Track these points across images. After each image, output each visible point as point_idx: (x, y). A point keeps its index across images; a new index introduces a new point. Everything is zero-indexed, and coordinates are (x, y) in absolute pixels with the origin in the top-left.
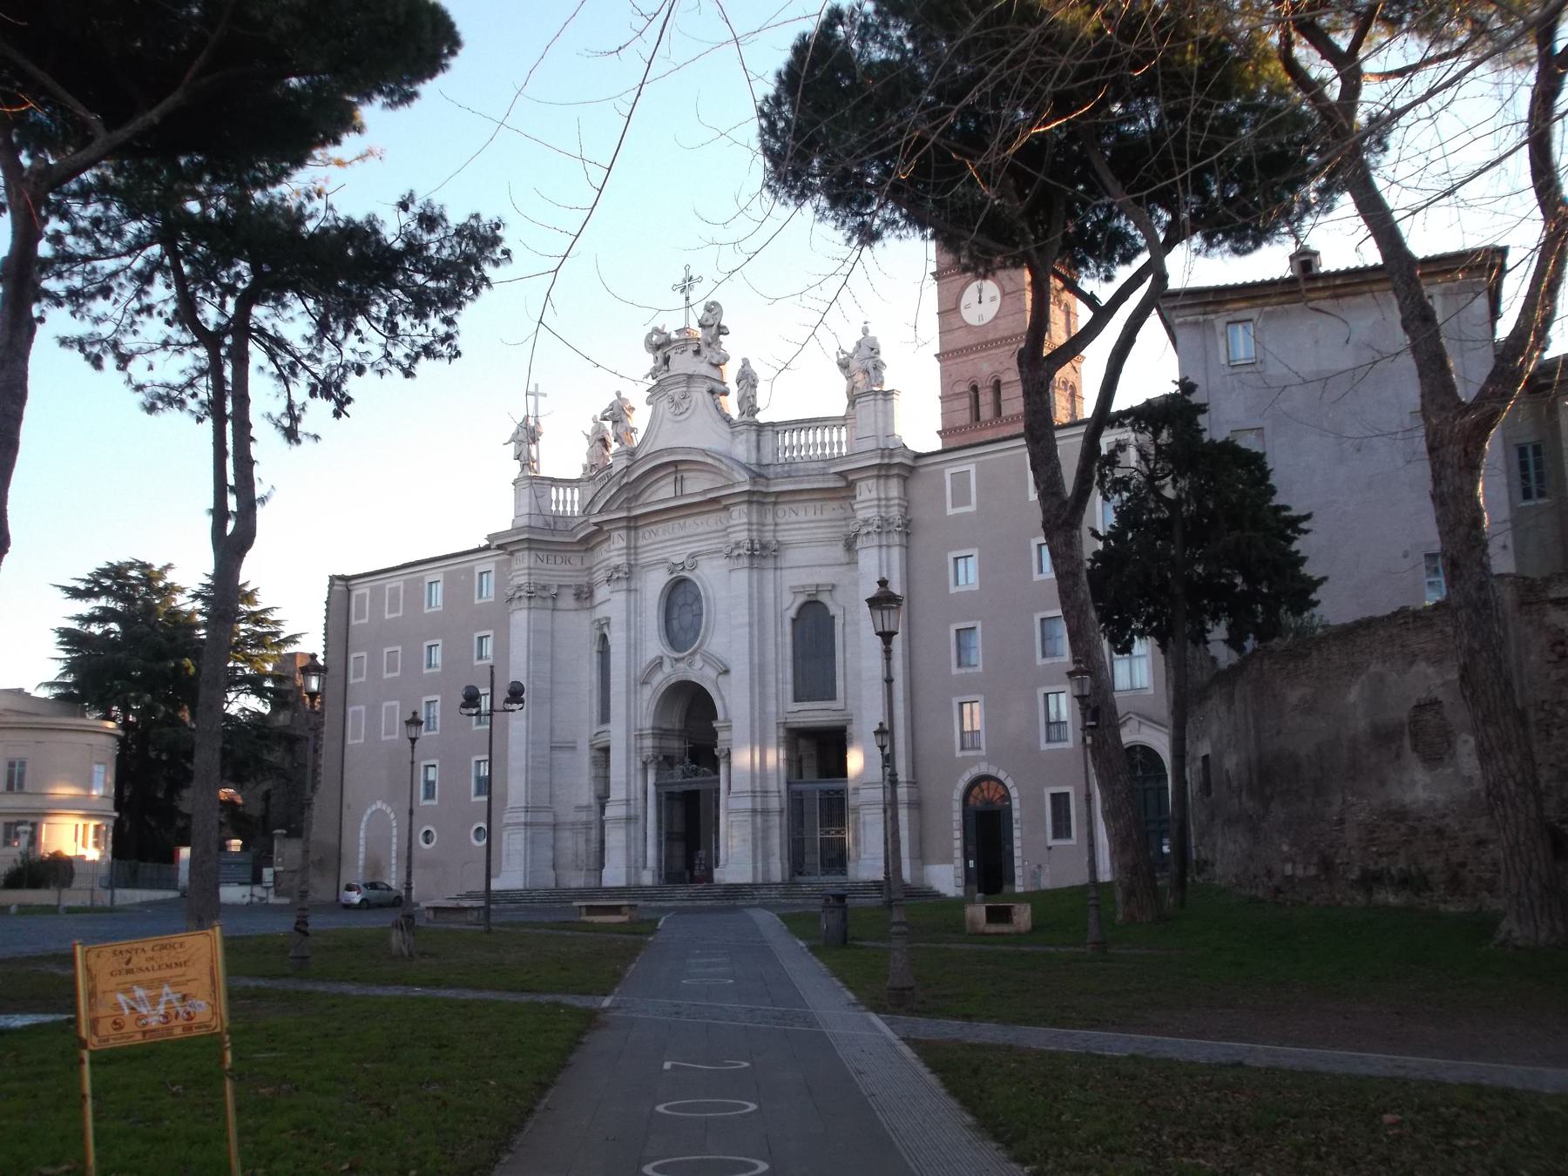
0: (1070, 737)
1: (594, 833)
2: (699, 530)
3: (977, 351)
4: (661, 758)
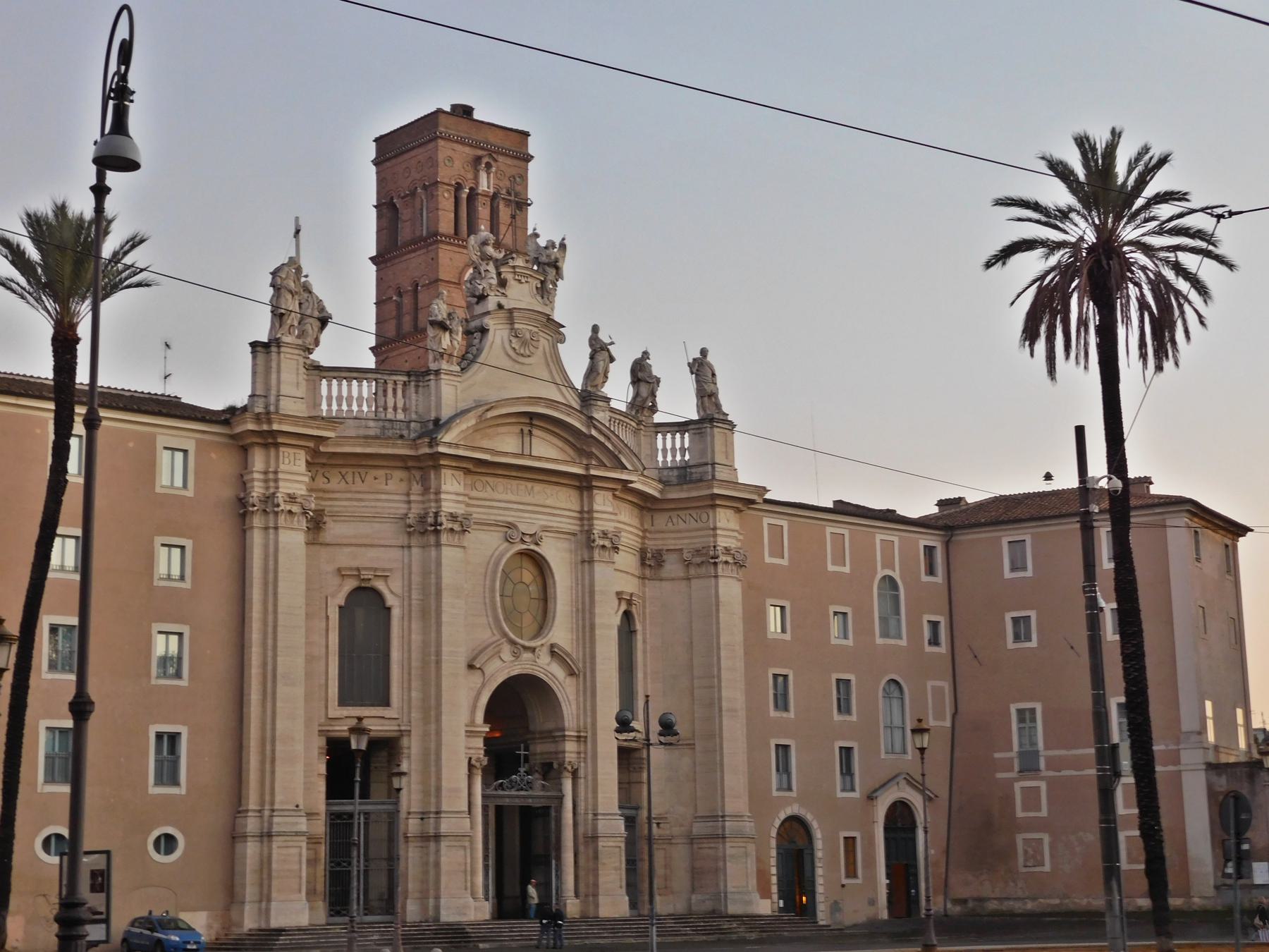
0: (857, 787)
2: (548, 502)
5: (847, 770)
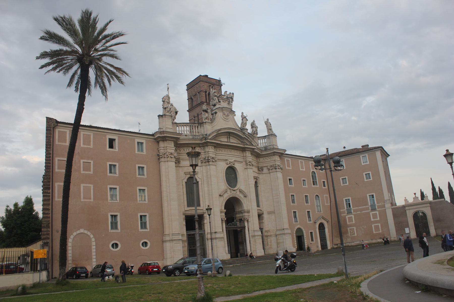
0: (312, 220)
2: (235, 154)
4: (235, 220)
5: (309, 217)
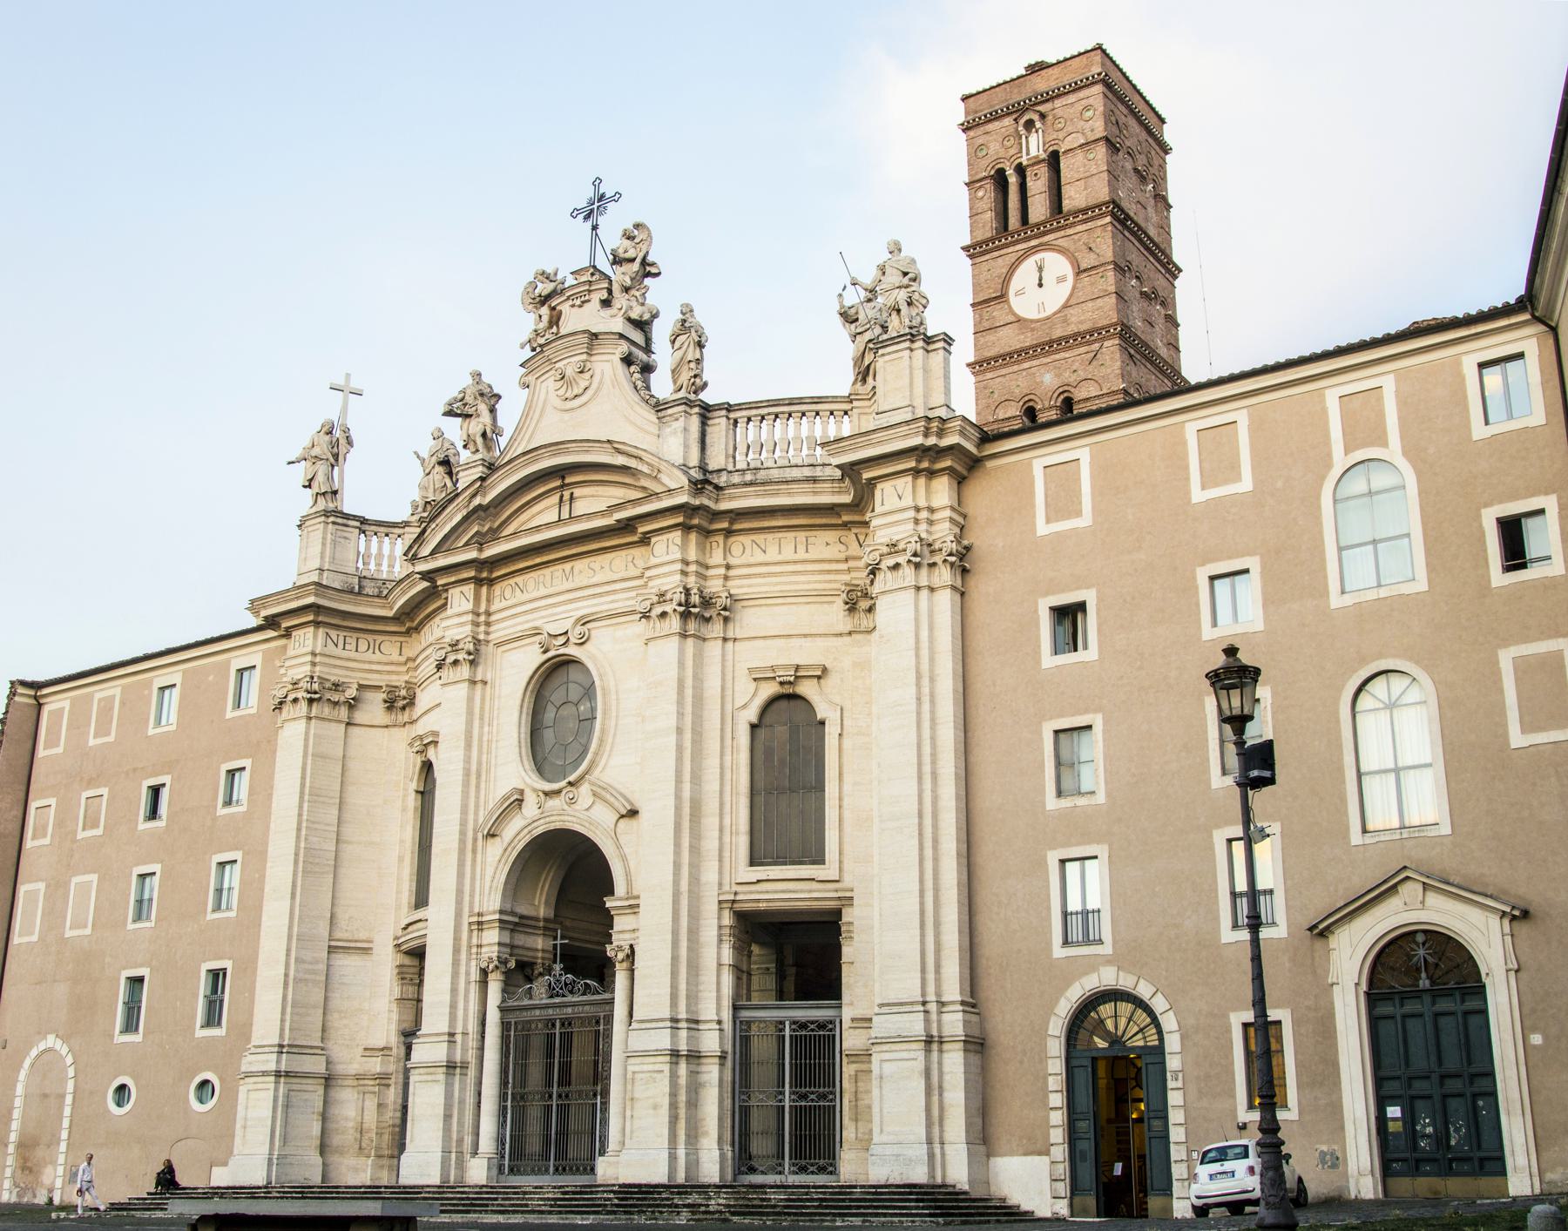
1: (392, 1095)
2: (594, 580)
3: (1035, 357)
4: (512, 964)
